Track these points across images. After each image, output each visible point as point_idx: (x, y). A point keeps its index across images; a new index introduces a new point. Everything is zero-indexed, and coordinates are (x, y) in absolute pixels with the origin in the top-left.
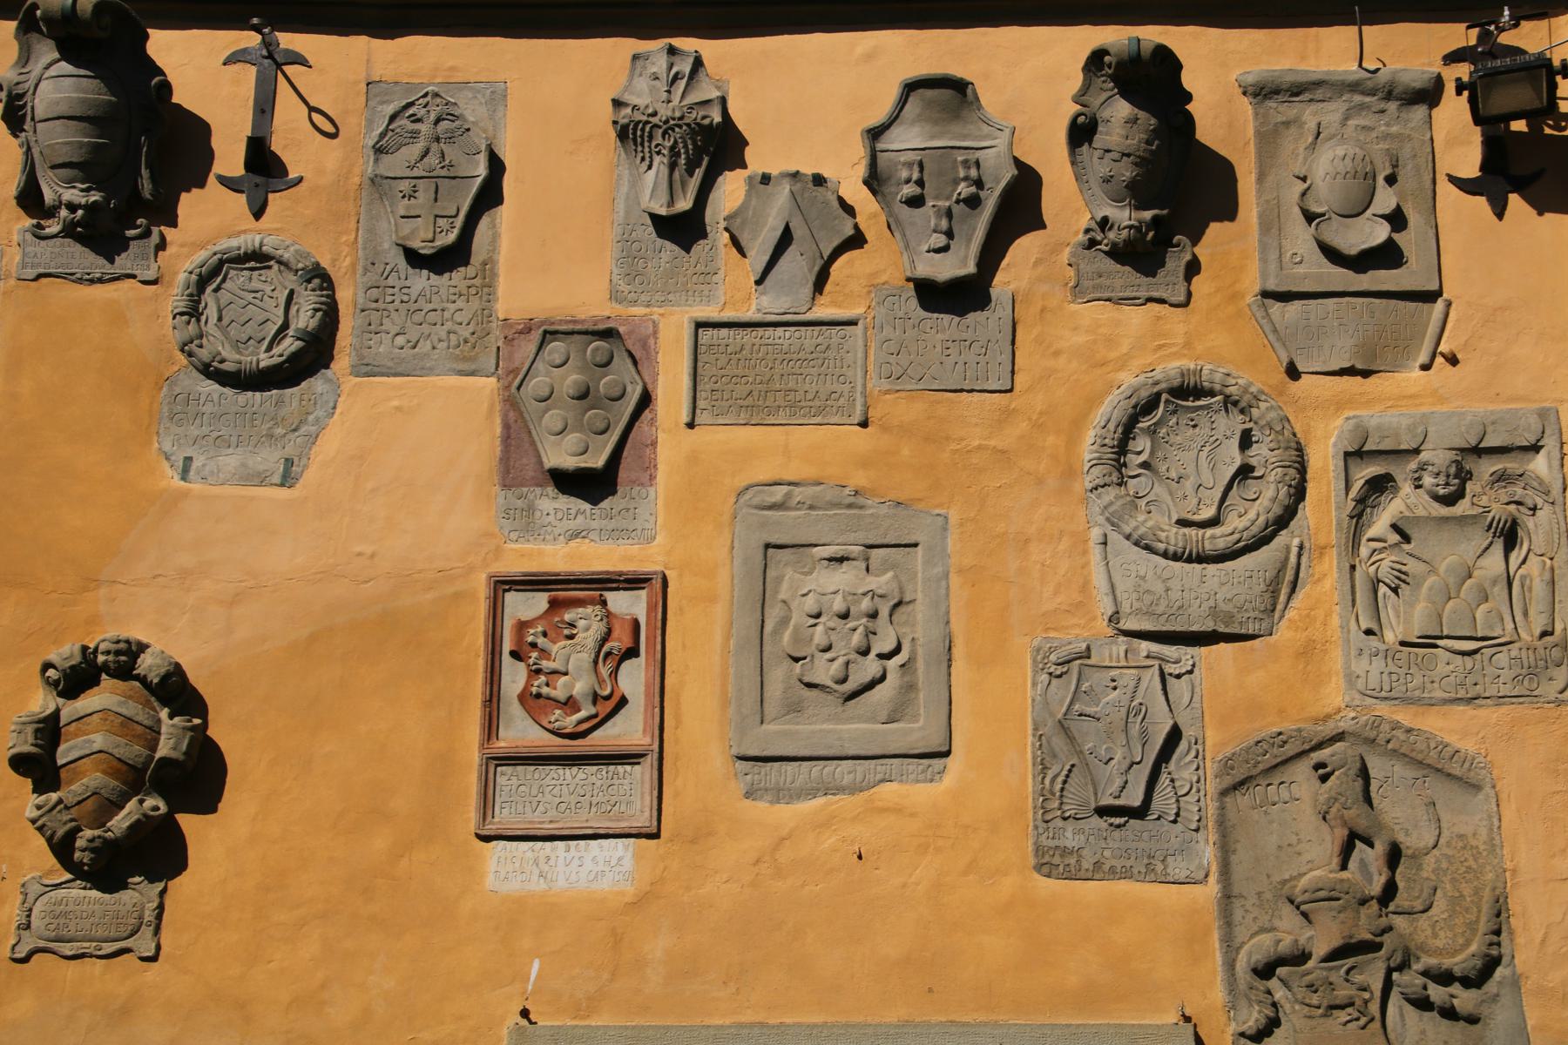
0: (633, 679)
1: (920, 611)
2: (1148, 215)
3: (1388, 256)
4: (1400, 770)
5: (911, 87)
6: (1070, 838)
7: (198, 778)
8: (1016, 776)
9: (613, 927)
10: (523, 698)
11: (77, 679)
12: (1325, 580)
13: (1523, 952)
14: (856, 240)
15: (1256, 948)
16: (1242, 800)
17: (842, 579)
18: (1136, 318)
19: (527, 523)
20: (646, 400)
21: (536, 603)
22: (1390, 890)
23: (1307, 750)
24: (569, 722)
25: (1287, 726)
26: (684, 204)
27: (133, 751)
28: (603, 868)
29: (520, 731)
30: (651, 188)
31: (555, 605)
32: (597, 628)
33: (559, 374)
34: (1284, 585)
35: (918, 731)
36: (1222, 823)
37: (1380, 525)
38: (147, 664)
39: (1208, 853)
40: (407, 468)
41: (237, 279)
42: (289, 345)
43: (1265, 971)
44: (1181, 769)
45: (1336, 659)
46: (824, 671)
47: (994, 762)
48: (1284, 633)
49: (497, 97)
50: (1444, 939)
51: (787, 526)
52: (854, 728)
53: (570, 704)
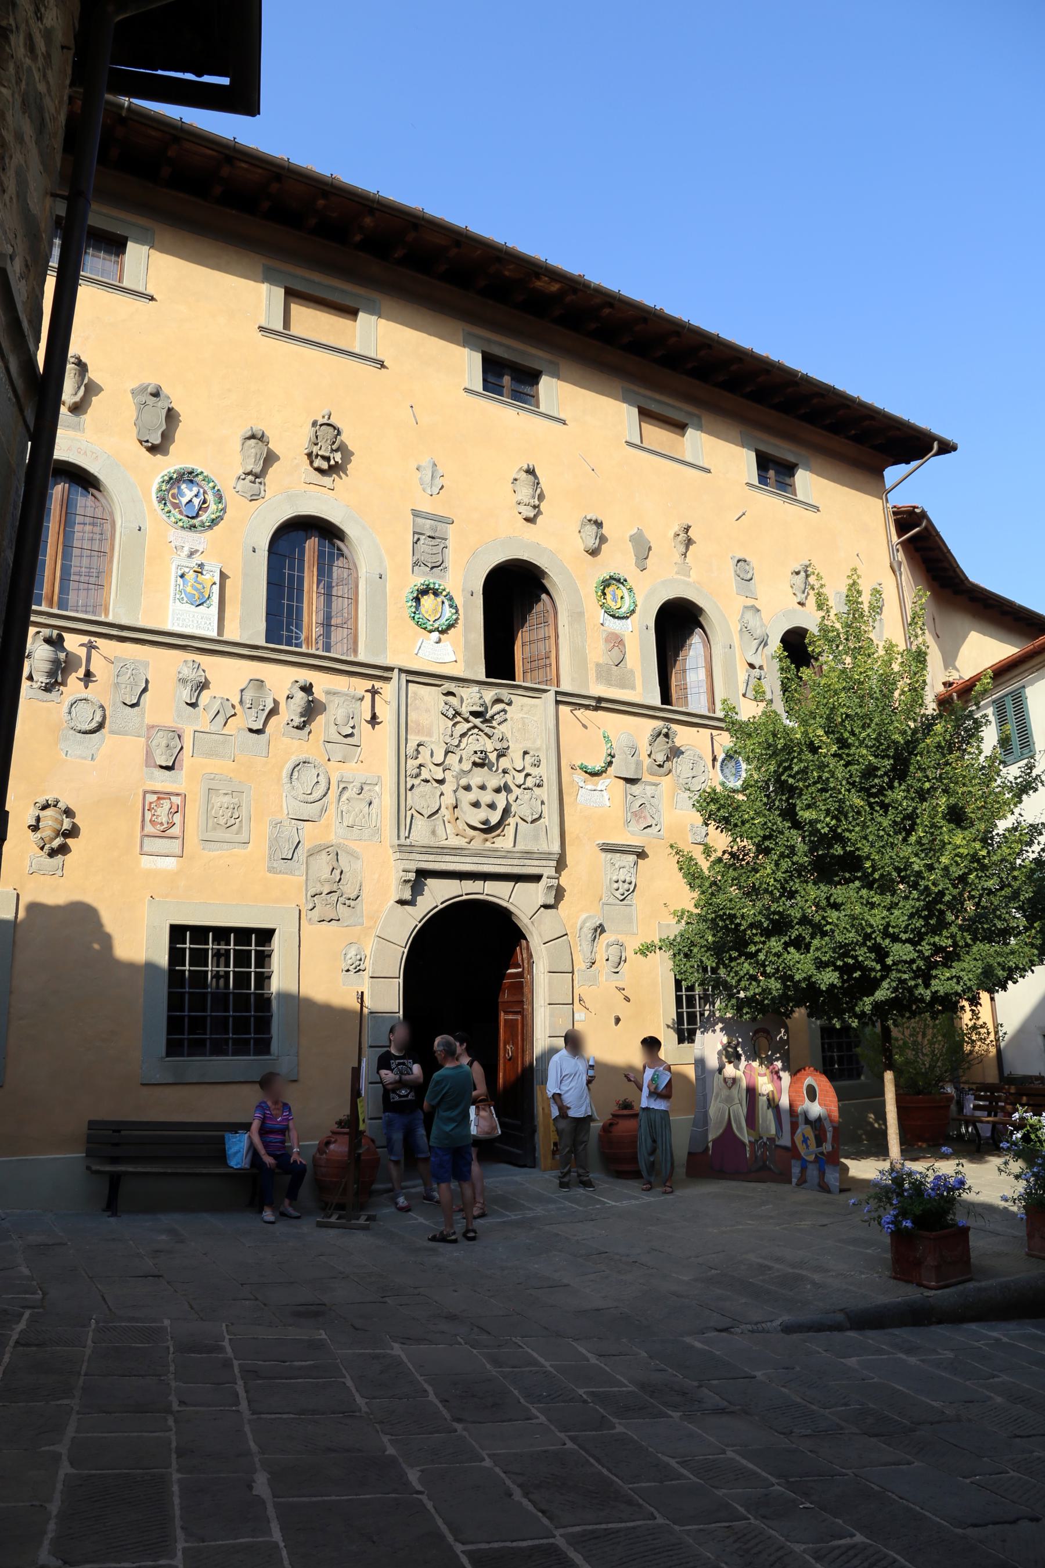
0: (177, 818)
2: (303, 719)
3: (351, 735)
6: (275, 865)
10: (150, 821)
11: (45, 807)
12: (332, 809)
13: (364, 895)
14: (235, 715)
16: (311, 858)
17: (226, 799)
18: (296, 742)
20: (182, 748)
21: (154, 797)
23: (325, 848)
24: (162, 828)
26: (194, 701)
27: (58, 827)
28: (169, 864)
29: (149, 829)
30: (186, 694)
31: (159, 798)
32: (169, 806)
33: (160, 740)
34: (324, 810)
37: (344, 798)
41: (81, 704)
42: (94, 725)
46: (222, 821)
47: (259, 847)
48: (323, 821)
49: (146, 665)
50: (350, 891)
52: (227, 835)
53: (162, 824)
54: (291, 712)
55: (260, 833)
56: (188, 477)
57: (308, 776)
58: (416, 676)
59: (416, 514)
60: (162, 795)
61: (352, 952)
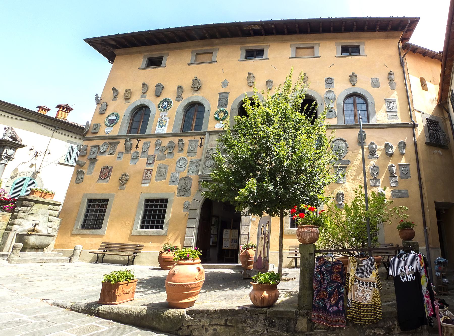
8: (169, 180)
9: (147, 188)
28: (147, 185)
29: (144, 178)
35: (164, 178)
40: (142, 163)
50: (188, 188)
52: (162, 178)
55: (168, 176)
56: (165, 100)
58: (211, 133)
59: (220, 94)
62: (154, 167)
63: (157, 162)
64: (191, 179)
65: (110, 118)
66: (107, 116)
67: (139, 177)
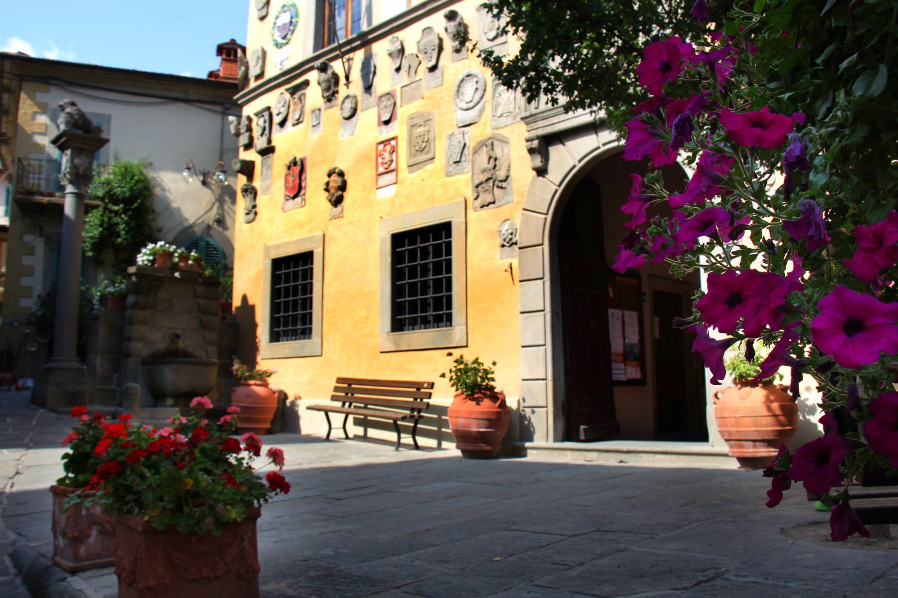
1: (432, 132)
4: (499, 143)
5: (423, 30)
7: (343, 187)
11: (329, 175)
13: (513, 174)
15: (477, 182)
19: (381, 132)
22: (495, 166)
24: (386, 166)
25: (481, 139)
35: (430, 156)
36: (473, 161)
38: (337, 171)
39: (470, 167)
43: (477, 187)
44: (466, 151)
45: (489, 124)
48: (482, 120)
50: (501, 174)
51: (415, 121)
54: (449, 44)
55: (441, 149)
57: (469, 89)
60: (385, 142)
61: (506, 226)
62: (398, 129)
63: (404, 112)
64: (504, 141)
65: (280, 23)
66: (273, 20)
67: (369, 172)
